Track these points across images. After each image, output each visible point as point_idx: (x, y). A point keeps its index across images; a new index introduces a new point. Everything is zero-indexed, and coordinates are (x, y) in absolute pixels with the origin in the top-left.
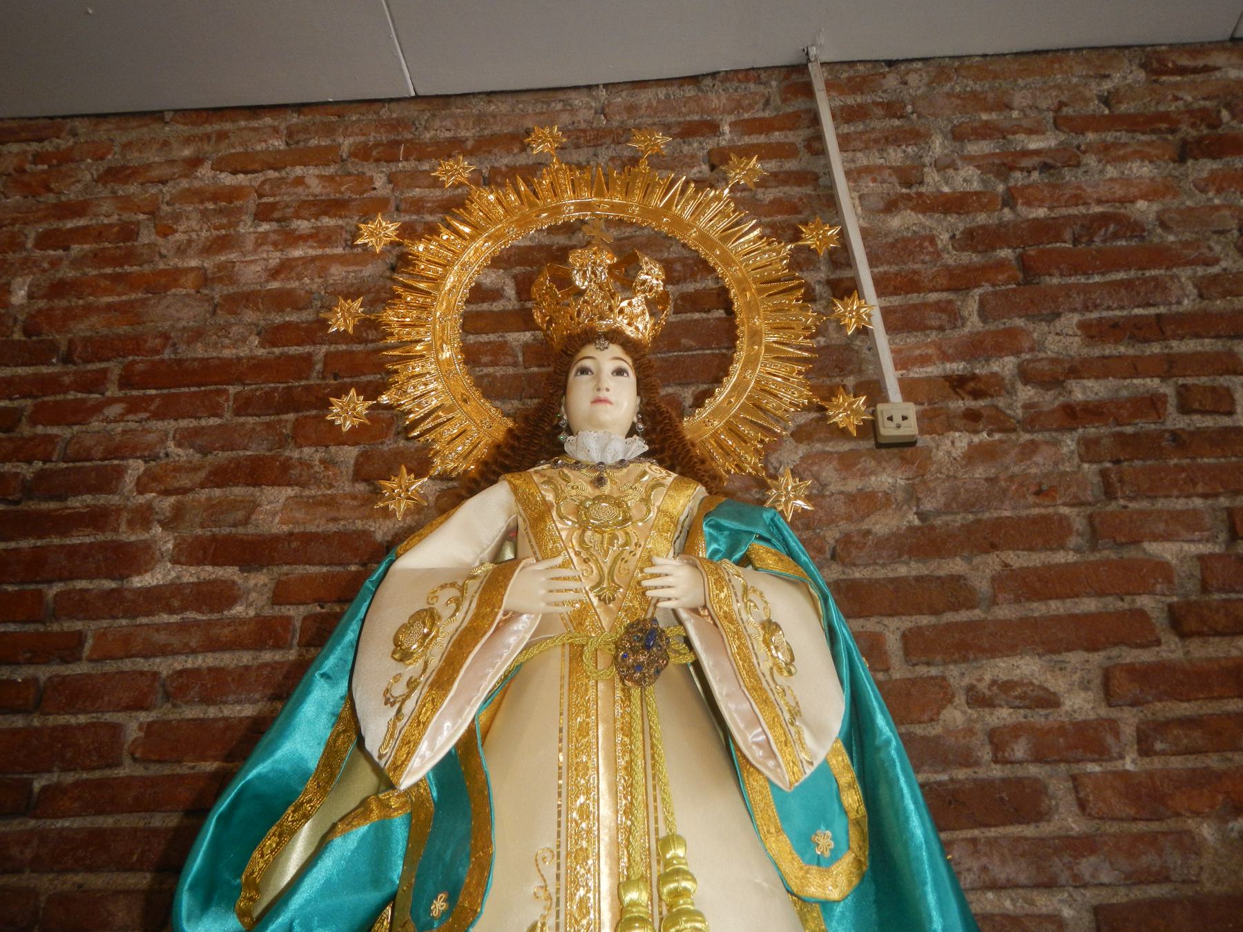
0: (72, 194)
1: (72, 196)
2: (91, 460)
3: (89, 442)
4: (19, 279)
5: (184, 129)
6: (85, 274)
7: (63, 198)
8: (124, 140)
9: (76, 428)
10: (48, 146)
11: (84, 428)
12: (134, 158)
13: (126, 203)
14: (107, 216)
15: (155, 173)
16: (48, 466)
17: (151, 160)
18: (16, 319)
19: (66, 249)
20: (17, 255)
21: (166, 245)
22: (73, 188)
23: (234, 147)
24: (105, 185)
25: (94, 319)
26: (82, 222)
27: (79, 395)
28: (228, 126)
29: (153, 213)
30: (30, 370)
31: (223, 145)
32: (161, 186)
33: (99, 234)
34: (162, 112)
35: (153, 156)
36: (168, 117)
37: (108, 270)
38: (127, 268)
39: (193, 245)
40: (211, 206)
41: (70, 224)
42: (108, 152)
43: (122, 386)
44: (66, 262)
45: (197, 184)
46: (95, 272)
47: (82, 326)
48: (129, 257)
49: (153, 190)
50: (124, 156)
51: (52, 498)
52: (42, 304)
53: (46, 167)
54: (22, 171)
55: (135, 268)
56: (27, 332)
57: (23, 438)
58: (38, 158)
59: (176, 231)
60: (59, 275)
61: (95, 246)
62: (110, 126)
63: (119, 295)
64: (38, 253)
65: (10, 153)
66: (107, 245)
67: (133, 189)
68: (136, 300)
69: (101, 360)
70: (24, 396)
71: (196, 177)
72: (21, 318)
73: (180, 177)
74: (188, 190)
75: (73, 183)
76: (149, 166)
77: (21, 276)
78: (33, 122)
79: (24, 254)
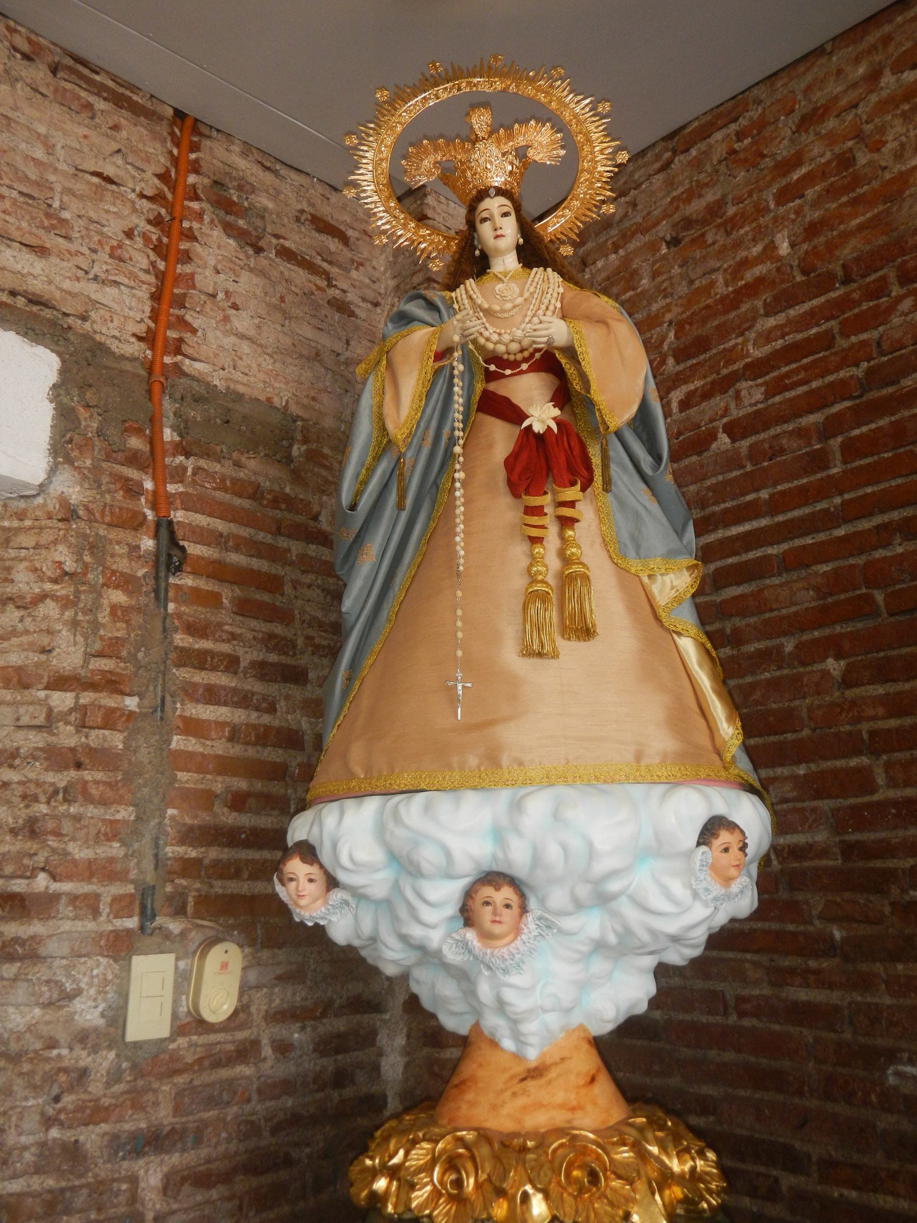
0: (783, 150)
1: (785, 153)
2: (905, 348)
3: (897, 335)
4: (779, 235)
5: (849, 51)
6: (827, 210)
7: (779, 158)
8: (803, 86)
9: (881, 329)
10: (743, 122)
11: (888, 326)
12: (819, 97)
13: (831, 139)
14: (822, 156)
15: (844, 102)
16: (872, 363)
17: (835, 92)
18: (791, 267)
19: (802, 196)
20: (767, 218)
21: (885, 157)
22: (781, 146)
23: (903, 45)
24: (806, 131)
25: (853, 242)
26: (804, 170)
27: (871, 304)
28: (887, 28)
29: (859, 136)
30: (822, 299)
31: (891, 49)
32: (854, 111)
33: (822, 173)
34: (822, 46)
35: (834, 88)
36: (829, 47)
37: (844, 199)
38: (859, 191)
39: (907, 146)
40: (906, 107)
41: (796, 176)
42: (795, 103)
43: (902, 284)
44: (806, 208)
45: (884, 94)
46: (835, 205)
47: (847, 251)
48: (856, 181)
49: (850, 117)
50: (810, 102)
51: (887, 385)
52: (805, 246)
53: (750, 140)
54: (733, 152)
55: (865, 188)
56: (805, 272)
57: (843, 350)
58: (740, 136)
59: (887, 142)
60: (808, 219)
61: (823, 184)
62: (785, 80)
63: (864, 214)
64: (782, 210)
65: (717, 142)
66: (832, 179)
67: (831, 123)
68: (880, 213)
69: (875, 271)
70: (827, 320)
71: (882, 89)
72: (795, 263)
73: (867, 94)
74: (880, 102)
75: (780, 142)
76: (836, 99)
77: (779, 232)
78: (722, 108)
79: (772, 215)
